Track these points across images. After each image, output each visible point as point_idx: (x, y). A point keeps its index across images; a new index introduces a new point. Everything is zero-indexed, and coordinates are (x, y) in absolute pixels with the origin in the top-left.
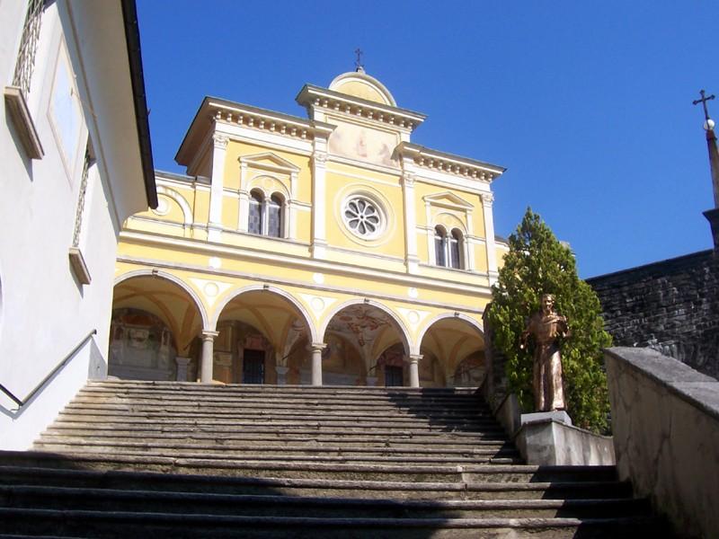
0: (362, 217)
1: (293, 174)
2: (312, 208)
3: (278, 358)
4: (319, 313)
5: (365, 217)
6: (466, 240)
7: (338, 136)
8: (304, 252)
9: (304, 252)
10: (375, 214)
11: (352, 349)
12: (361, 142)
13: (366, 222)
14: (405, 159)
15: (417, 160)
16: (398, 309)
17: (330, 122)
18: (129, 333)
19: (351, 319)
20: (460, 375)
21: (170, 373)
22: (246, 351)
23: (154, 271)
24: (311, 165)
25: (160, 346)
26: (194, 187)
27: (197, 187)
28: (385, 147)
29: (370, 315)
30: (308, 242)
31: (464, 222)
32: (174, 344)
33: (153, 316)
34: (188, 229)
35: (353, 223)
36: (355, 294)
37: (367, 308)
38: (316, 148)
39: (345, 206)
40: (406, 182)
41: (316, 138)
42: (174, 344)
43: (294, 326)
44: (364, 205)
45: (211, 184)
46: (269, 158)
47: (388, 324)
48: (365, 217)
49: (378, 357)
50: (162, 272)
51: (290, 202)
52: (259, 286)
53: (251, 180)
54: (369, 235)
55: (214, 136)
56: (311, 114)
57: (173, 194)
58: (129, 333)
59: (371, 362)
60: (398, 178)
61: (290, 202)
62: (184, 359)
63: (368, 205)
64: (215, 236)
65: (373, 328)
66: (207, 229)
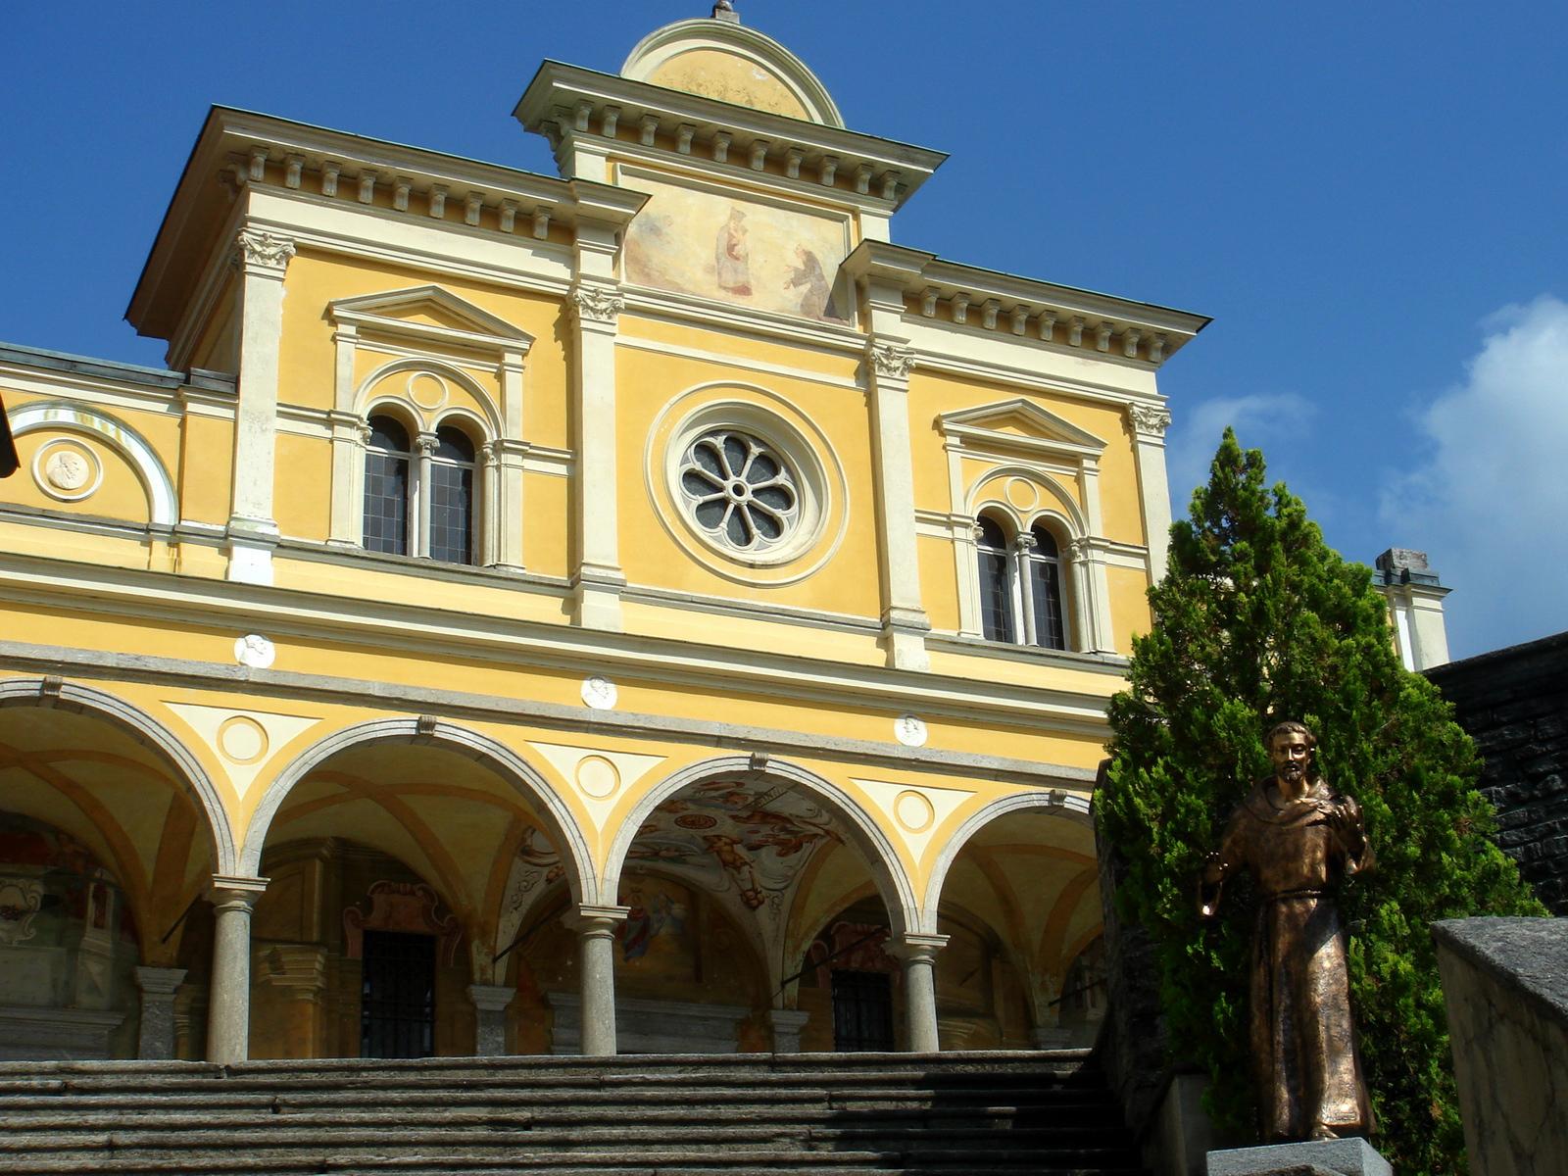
0: (738, 490)
1: (509, 358)
2: (573, 458)
3: (479, 958)
4: (601, 801)
5: (749, 488)
7: (654, 230)
8: (549, 609)
9: (549, 609)
10: (782, 479)
11: (722, 919)
12: (731, 248)
13: (750, 506)
16: (865, 787)
17: (626, 182)
19: (711, 822)
20: (1079, 995)
21: (117, 1020)
22: (371, 938)
23: (46, 685)
24: (567, 330)
25: (83, 928)
26: (179, 405)
27: (191, 407)
28: (811, 260)
29: (774, 806)
30: (561, 576)
32: (128, 924)
33: (57, 832)
34: (160, 546)
35: (709, 512)
36: (719, 741)
37: (764, 787)
38: (584, 270)
39: (678, 457)
41: (580, 241)
42: (128, 924)
43: (527, 852)
45: (236, 392)
46: (430, 305)
47: (841, 835)
48: (749, 488)
49: (806, 946)
50: (73, 688)
51: (499, 448)
52: (403, 723)
53: (363, 380)
54: (764, 548)
55: (246, 236)
56: (564, 159)
57: (111, 431)
59: (783, 963)
60: (854, 363)
61: (499, 448)
62: (167, 973)
63: (755, 450)
64: (252, 566)
65: (787, 848)
66: (224, 542)
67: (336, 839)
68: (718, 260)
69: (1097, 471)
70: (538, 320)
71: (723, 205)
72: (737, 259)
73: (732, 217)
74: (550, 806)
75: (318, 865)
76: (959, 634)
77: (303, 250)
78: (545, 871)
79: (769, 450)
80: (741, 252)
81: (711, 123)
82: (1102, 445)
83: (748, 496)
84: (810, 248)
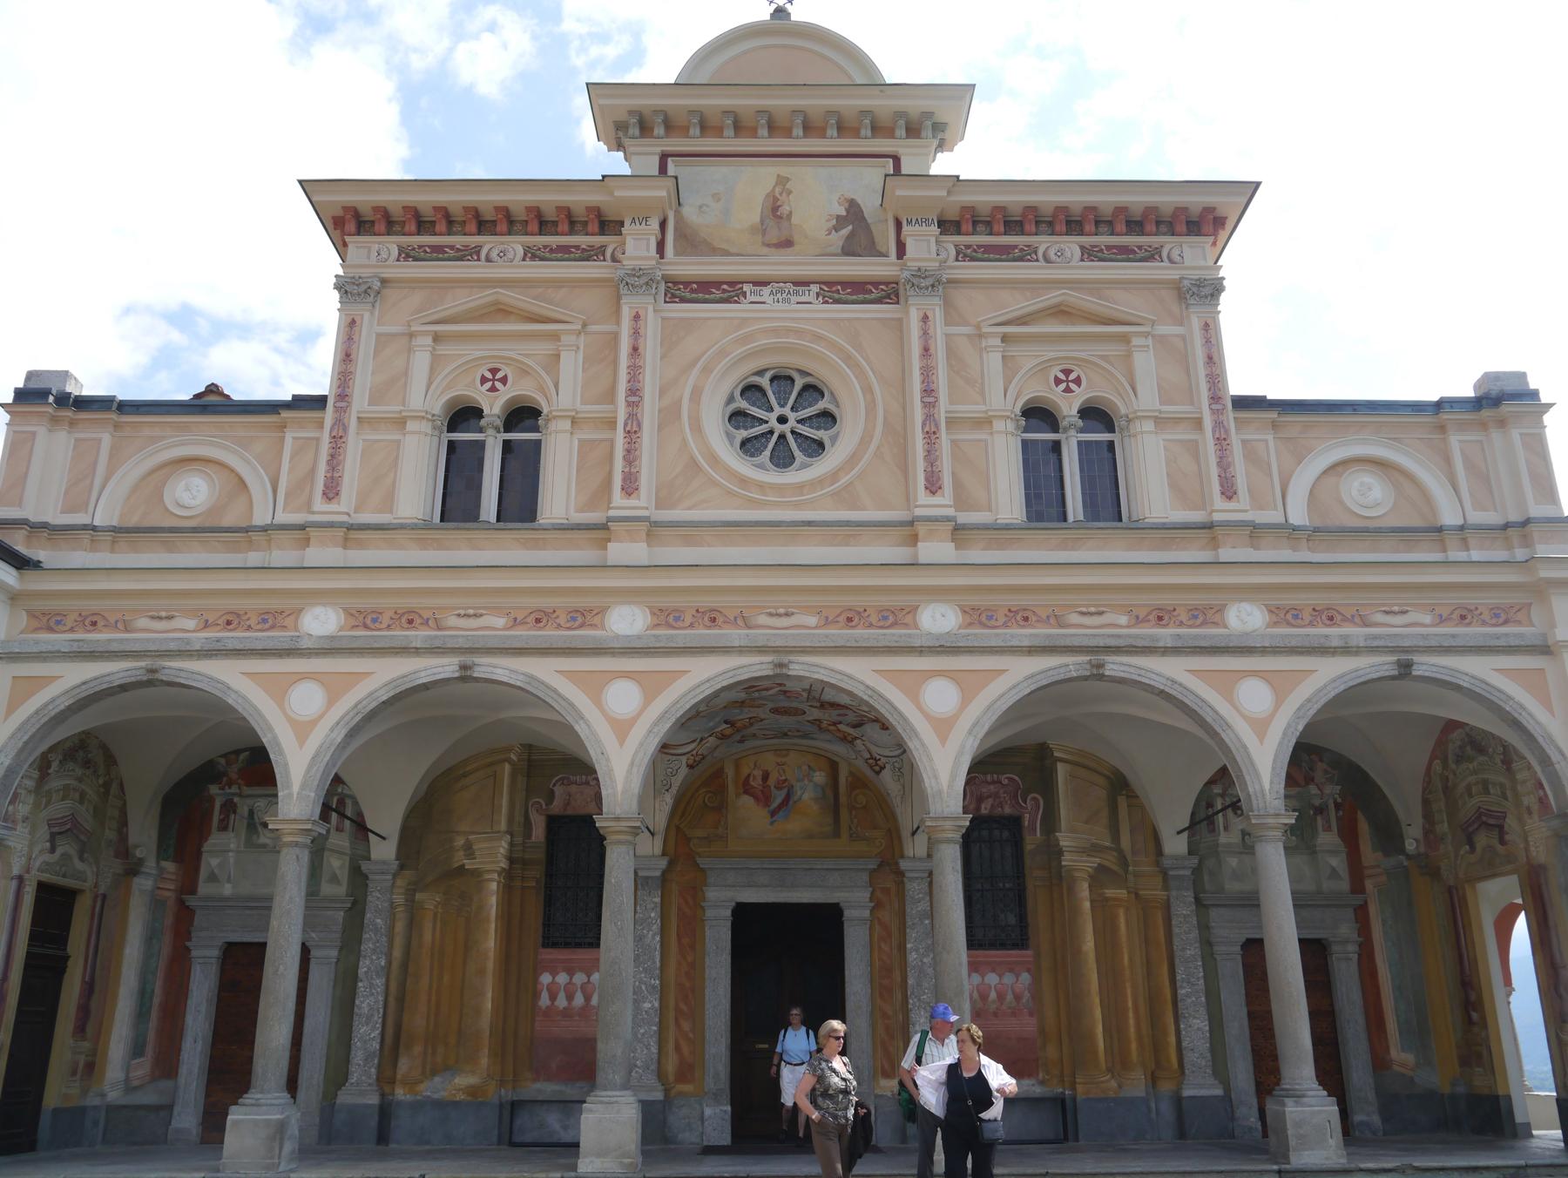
0: (782, 420)
11: (858, 782)
18: (251, 813)
20: (1210, 820)
22: (553, 822)
52: (445, 667)
58: (251, 813)
67: (529, 748)
74: (577, 727)
75: (507, 767)
78: (684, 759)
83: (792, 423)
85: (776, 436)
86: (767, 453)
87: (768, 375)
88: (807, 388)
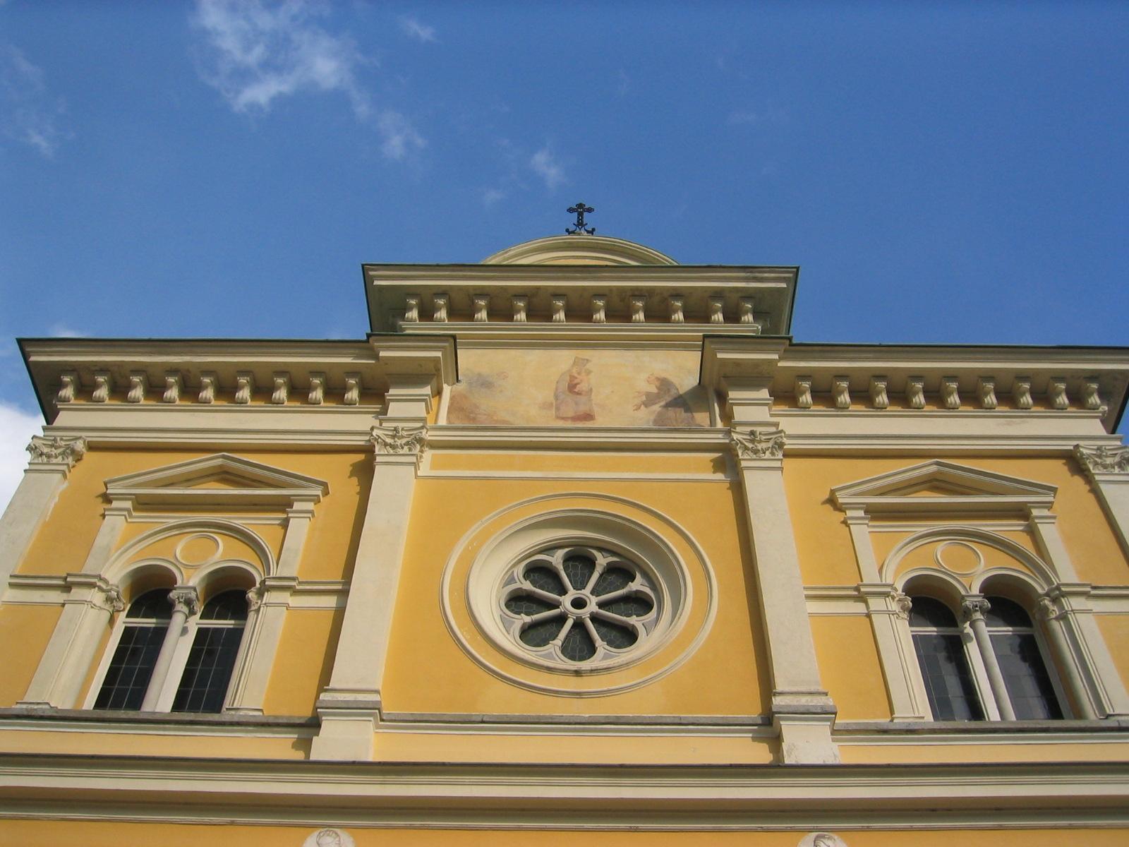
0: (579, 603)
6: (1054, 610)
10: (638, 584)
12: (572, 388)
14: (733, 395)
15: (785, 396)
31: (1025, 543)
40: (746, 460)
44: (590, 563)
46: (224, 475)
63: (602, 561)
68: (556, 397)
69: (1054, 517)
70: (336, 470)
71: (563, 359)
72: (578, 394)
73: (574, 363)
76: (892, 721)
77: (92, 447)
79: (623, 560)
80: (584, 389)
81: (538, 288)
82: (1054, 490)
84: (664, 375)
85: (570, 623)
86: (558, 642)
87: (560, 554)
88: (611, 570)
